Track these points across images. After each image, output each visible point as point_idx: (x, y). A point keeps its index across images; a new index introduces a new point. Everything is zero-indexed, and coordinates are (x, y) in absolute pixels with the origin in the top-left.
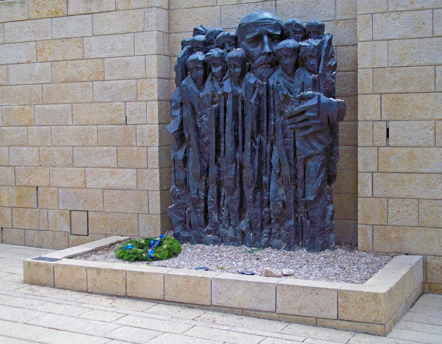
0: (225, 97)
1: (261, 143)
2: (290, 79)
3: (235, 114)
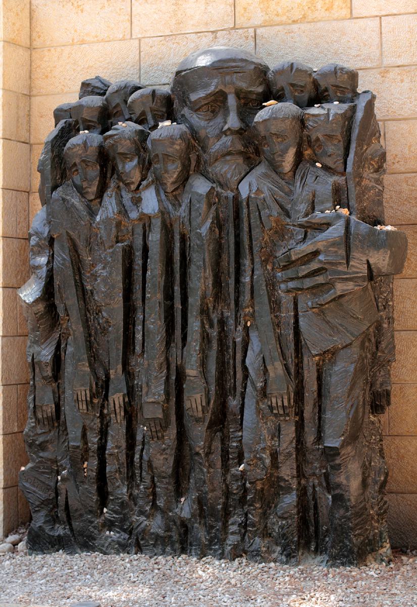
1: (222, 322)
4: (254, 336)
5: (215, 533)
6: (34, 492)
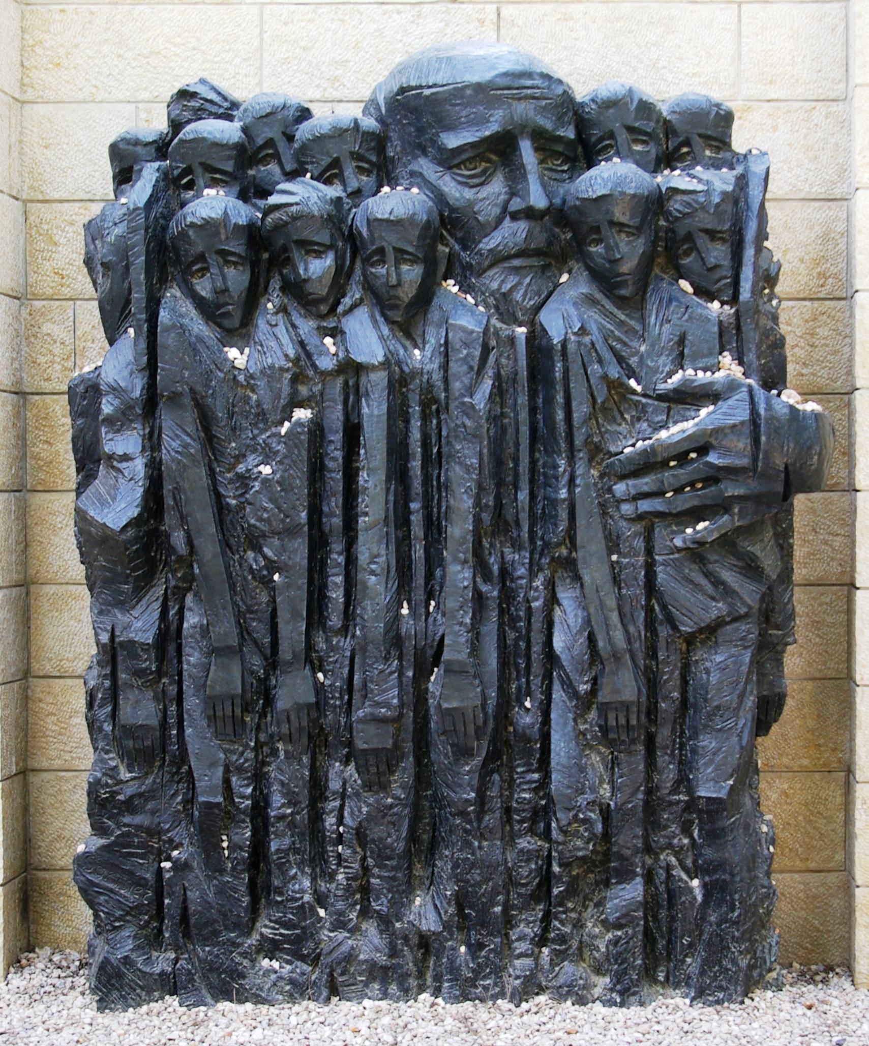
0: (346, 383)
1: (505, 573)
2: (623, 317)
3: (398, 452)
4: (567, 595)
5: (487, 958)
6: (111, 891)
